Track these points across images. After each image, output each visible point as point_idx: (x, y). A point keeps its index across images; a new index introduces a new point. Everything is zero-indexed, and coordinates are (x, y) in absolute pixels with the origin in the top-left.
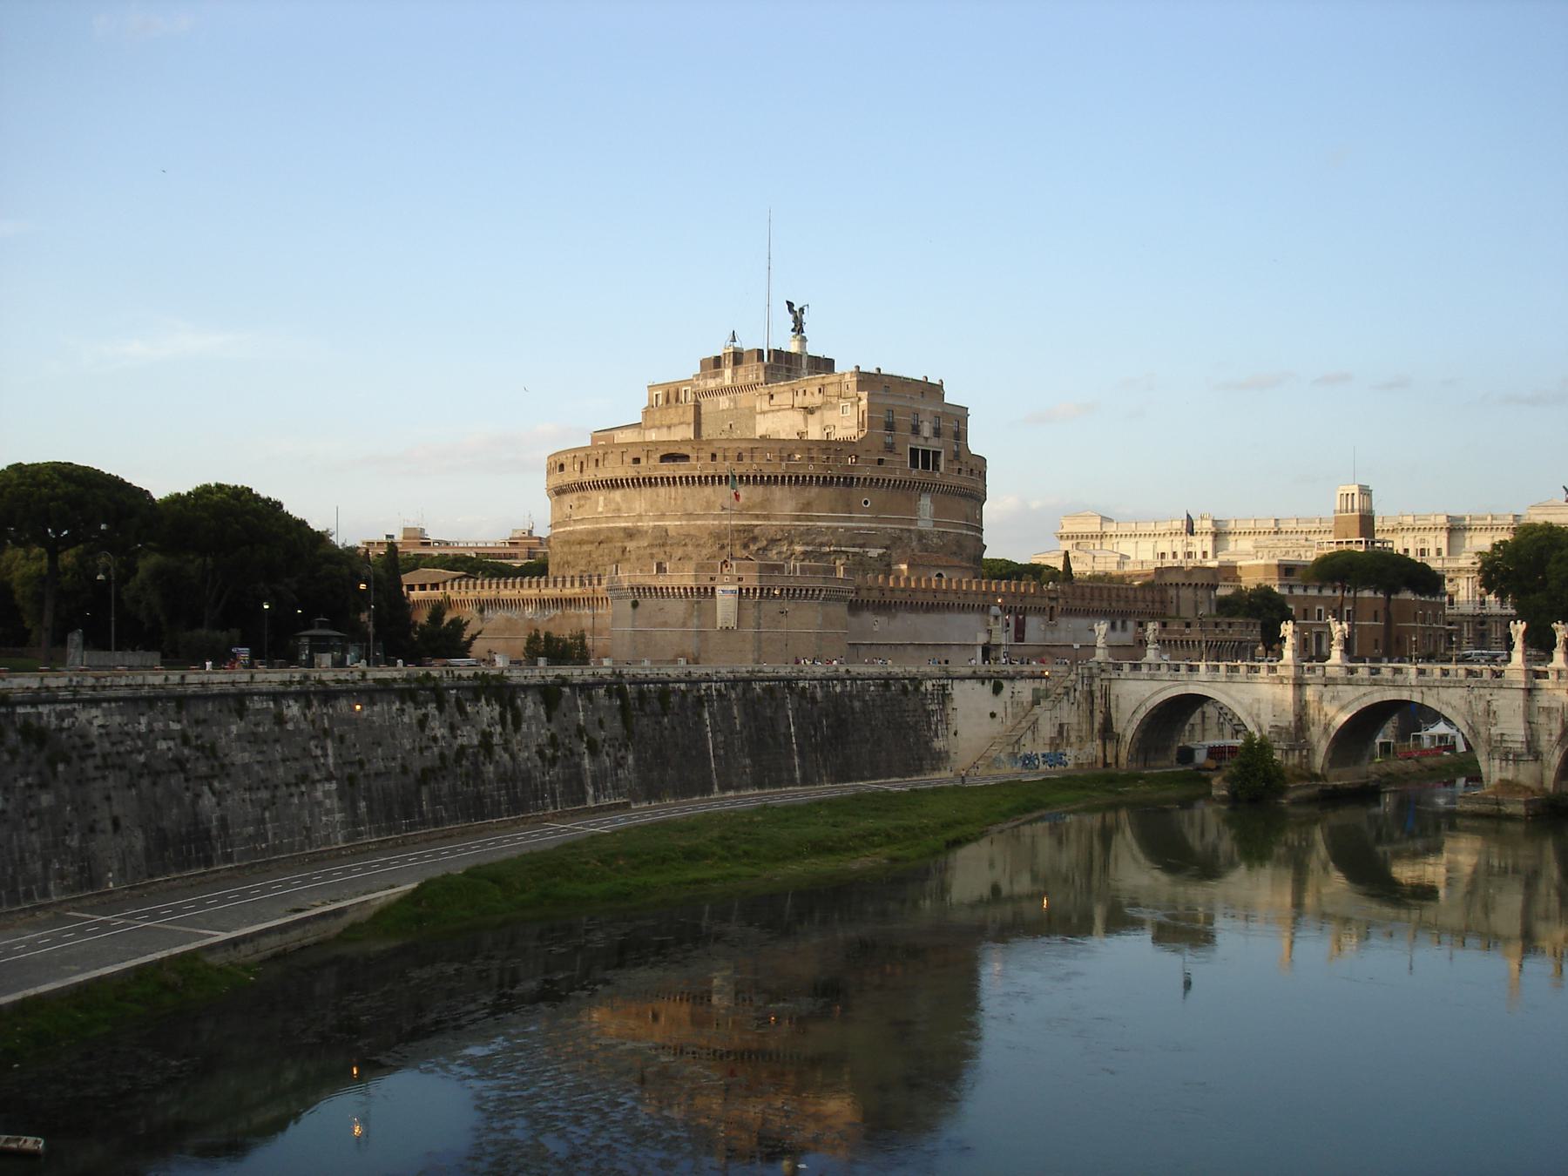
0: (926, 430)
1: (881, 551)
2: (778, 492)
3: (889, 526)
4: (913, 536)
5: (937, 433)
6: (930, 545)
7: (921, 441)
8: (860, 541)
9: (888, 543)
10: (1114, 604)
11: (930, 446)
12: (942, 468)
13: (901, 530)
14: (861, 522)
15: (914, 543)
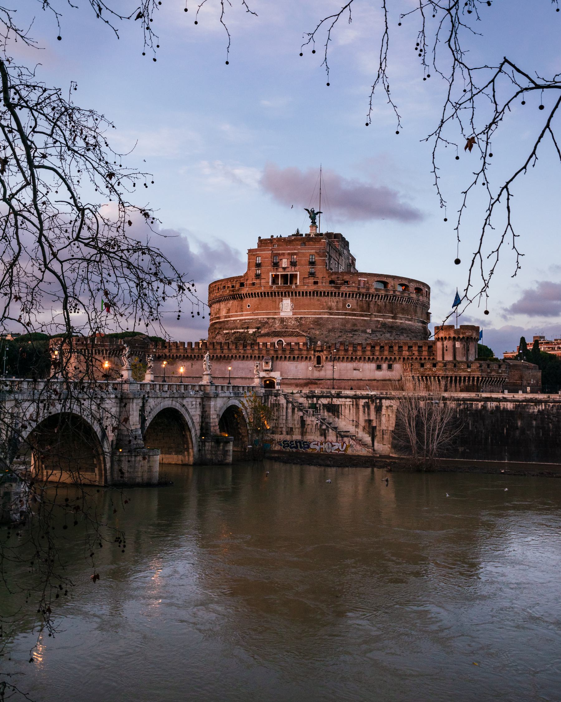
0: (285, 263)
1: (254, 330)
2: (223, 305)
3: (260, 317)
4: (277, 321)
5: (293, 264)
6: (290, 326)
7: (280, 270)
8: (245, 326)
9: (259, 325)
10: (377, 353)
11: (288, 272)
12: (298, 284)
13: (268, 318)
14: (246, 316)
15: (277, 324)
